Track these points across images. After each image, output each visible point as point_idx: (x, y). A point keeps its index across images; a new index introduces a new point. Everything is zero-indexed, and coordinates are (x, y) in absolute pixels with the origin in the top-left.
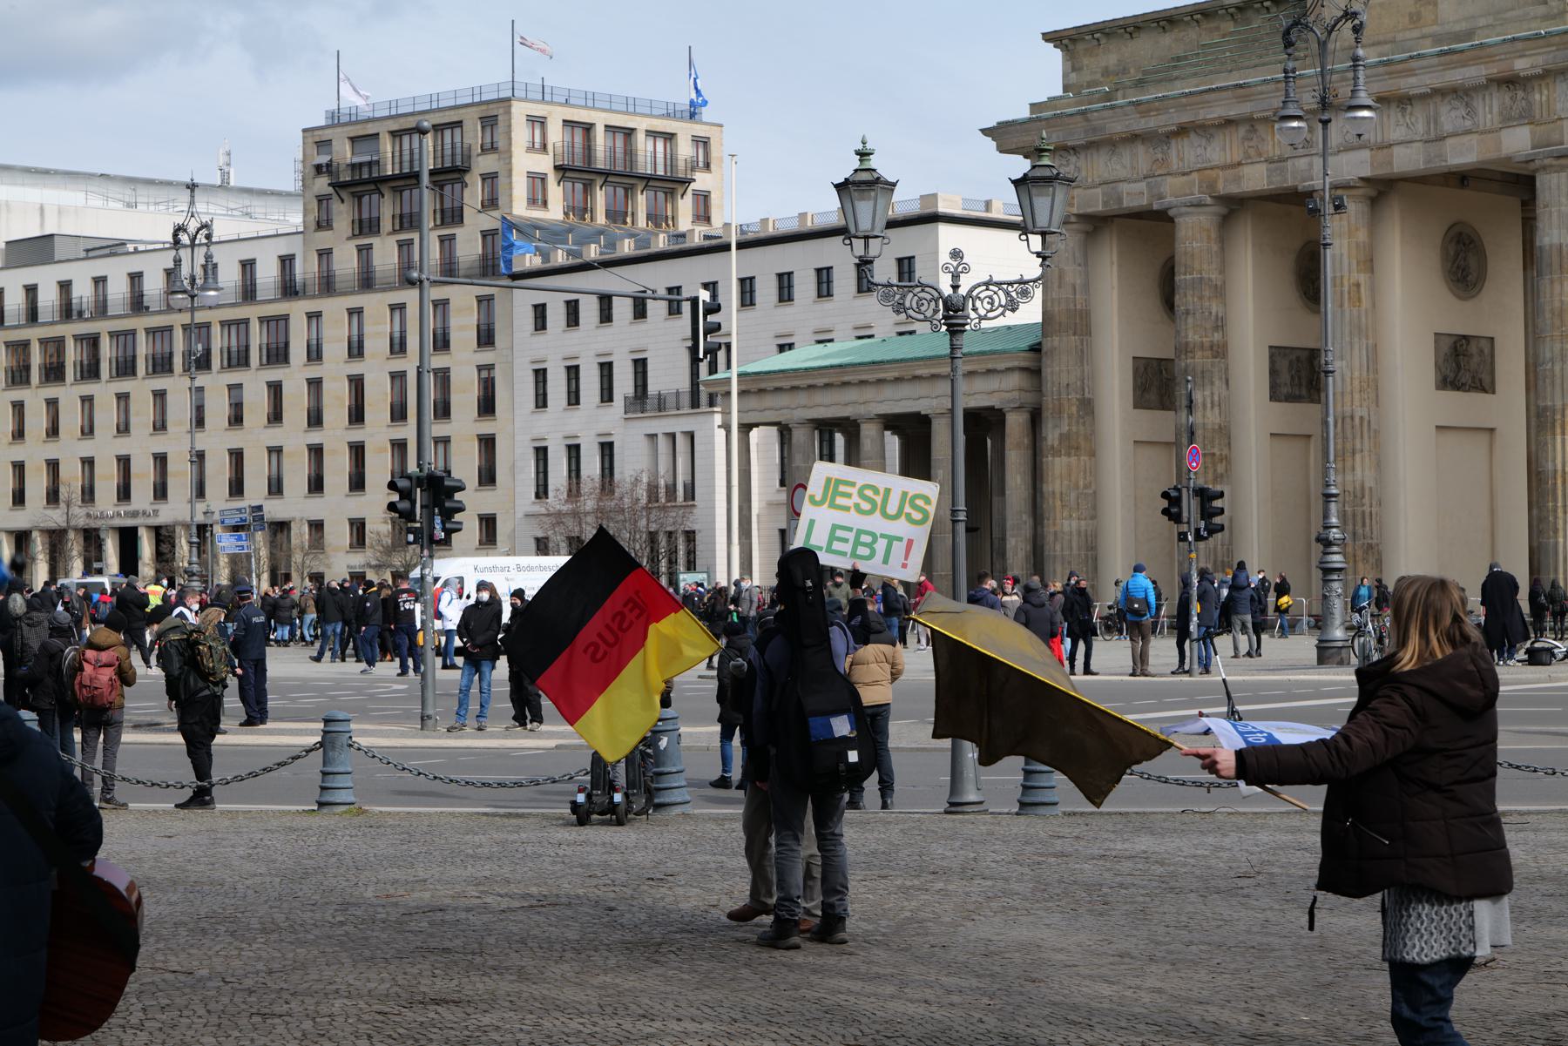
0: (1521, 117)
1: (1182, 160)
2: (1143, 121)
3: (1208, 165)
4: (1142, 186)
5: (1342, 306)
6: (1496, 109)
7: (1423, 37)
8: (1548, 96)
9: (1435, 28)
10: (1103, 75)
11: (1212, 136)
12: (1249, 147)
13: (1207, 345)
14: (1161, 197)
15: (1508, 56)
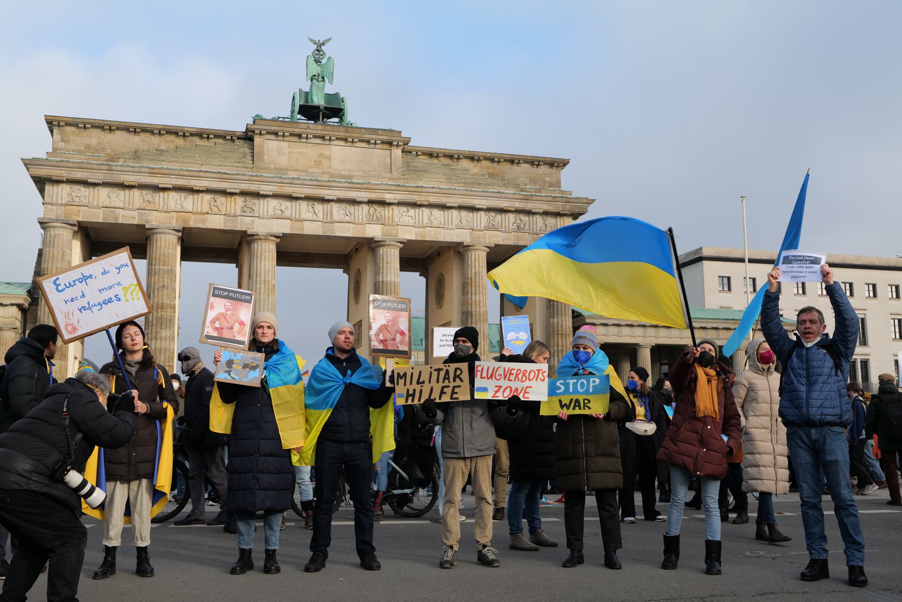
2: (150, 178)
3: (185, 210)
4: (135, 213)
5: (268, 295)
6: (364, 215)
7: (324, 173)
9: (330, 170)
10: (85, 148)
12: (214, 206)
13: (172, 306)
14: (148, 222)
15: (383, 191)
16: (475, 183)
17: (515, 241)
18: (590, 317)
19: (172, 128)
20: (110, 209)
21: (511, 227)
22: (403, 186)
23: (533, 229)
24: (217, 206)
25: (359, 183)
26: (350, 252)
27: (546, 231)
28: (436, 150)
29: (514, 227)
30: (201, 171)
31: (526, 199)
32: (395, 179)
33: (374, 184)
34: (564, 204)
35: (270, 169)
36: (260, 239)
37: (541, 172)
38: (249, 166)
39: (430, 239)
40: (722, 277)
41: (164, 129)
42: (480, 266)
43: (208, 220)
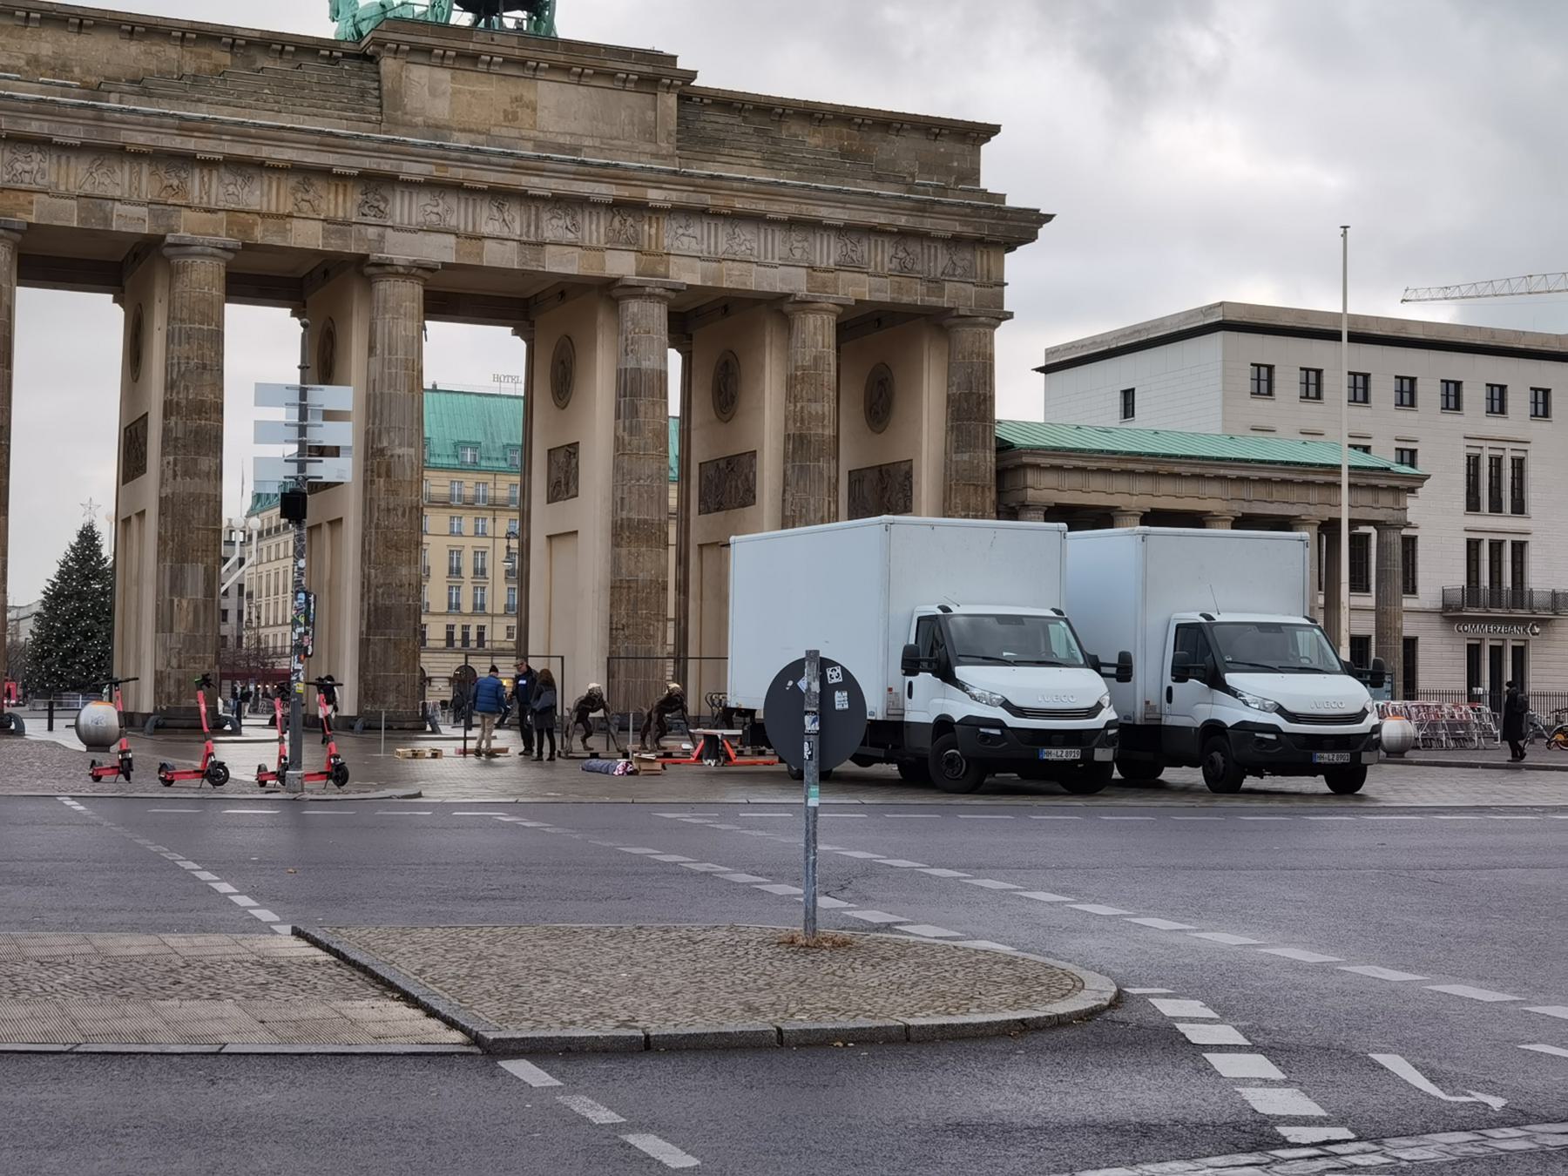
0: (628, 242)
1: (208, 194)
2: (178, 139)
3: (247, 208)
4: (143, 211)
5: (413, 390)
6: (602, 230)
7: (522, 138)
8: (657, 229)
9: (533, 134)
10: (28, 64)
11: (251, 177)
15: (644, 184)
16: (820, 172)
17: (895, 295)
18: (1034, 451)
19: (206, 28)
20: (93, 200)
21: (887, 265)
22: (684, 175)
23: (929, 270)
24: (309, 201)
25: (600, 165)
26: (536, 295)
27: (954, 275)
28: (741, 97)
29: (891, 266)
30: (283, 128)
31: (923, 208)
32: (664, 157)
33: (626, 168)
34: (993, 221)
35: (416, 126)
36: (397, 274)
37: (942, 150)
38: (374, 118)
39: (731, 286)
40: (1259, 366)
41: (192, 30)
42: (826, 344)
43: (291, 229)
